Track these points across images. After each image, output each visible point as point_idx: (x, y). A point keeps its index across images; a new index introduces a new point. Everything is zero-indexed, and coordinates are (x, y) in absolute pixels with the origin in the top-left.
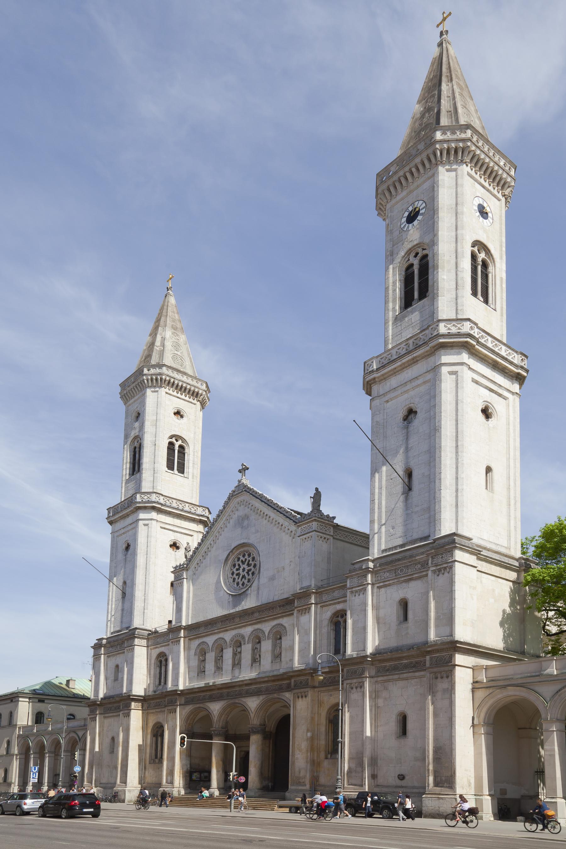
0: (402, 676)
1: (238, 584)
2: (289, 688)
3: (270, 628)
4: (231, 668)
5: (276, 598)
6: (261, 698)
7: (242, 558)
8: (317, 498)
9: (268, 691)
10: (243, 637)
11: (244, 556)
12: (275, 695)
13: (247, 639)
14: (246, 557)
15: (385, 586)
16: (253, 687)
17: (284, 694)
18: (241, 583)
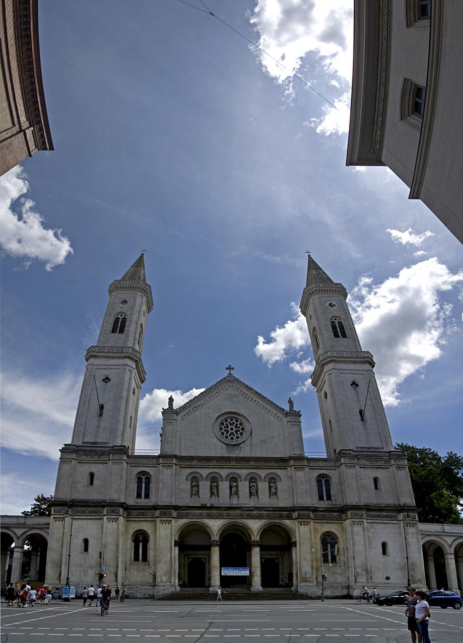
0: (383, 521)
1: (227, 437)
2: (289, 517)
3: (265, 474)
4: (229, 496)
6: (263, 521)
7: (229, 421)
9: (268, 517)
10: (240, 476)
11: (232, 420)
12: (277, 521)
13: (243, 478)
14: (234, 421)
15: (364, 468)
18: (229, 437)
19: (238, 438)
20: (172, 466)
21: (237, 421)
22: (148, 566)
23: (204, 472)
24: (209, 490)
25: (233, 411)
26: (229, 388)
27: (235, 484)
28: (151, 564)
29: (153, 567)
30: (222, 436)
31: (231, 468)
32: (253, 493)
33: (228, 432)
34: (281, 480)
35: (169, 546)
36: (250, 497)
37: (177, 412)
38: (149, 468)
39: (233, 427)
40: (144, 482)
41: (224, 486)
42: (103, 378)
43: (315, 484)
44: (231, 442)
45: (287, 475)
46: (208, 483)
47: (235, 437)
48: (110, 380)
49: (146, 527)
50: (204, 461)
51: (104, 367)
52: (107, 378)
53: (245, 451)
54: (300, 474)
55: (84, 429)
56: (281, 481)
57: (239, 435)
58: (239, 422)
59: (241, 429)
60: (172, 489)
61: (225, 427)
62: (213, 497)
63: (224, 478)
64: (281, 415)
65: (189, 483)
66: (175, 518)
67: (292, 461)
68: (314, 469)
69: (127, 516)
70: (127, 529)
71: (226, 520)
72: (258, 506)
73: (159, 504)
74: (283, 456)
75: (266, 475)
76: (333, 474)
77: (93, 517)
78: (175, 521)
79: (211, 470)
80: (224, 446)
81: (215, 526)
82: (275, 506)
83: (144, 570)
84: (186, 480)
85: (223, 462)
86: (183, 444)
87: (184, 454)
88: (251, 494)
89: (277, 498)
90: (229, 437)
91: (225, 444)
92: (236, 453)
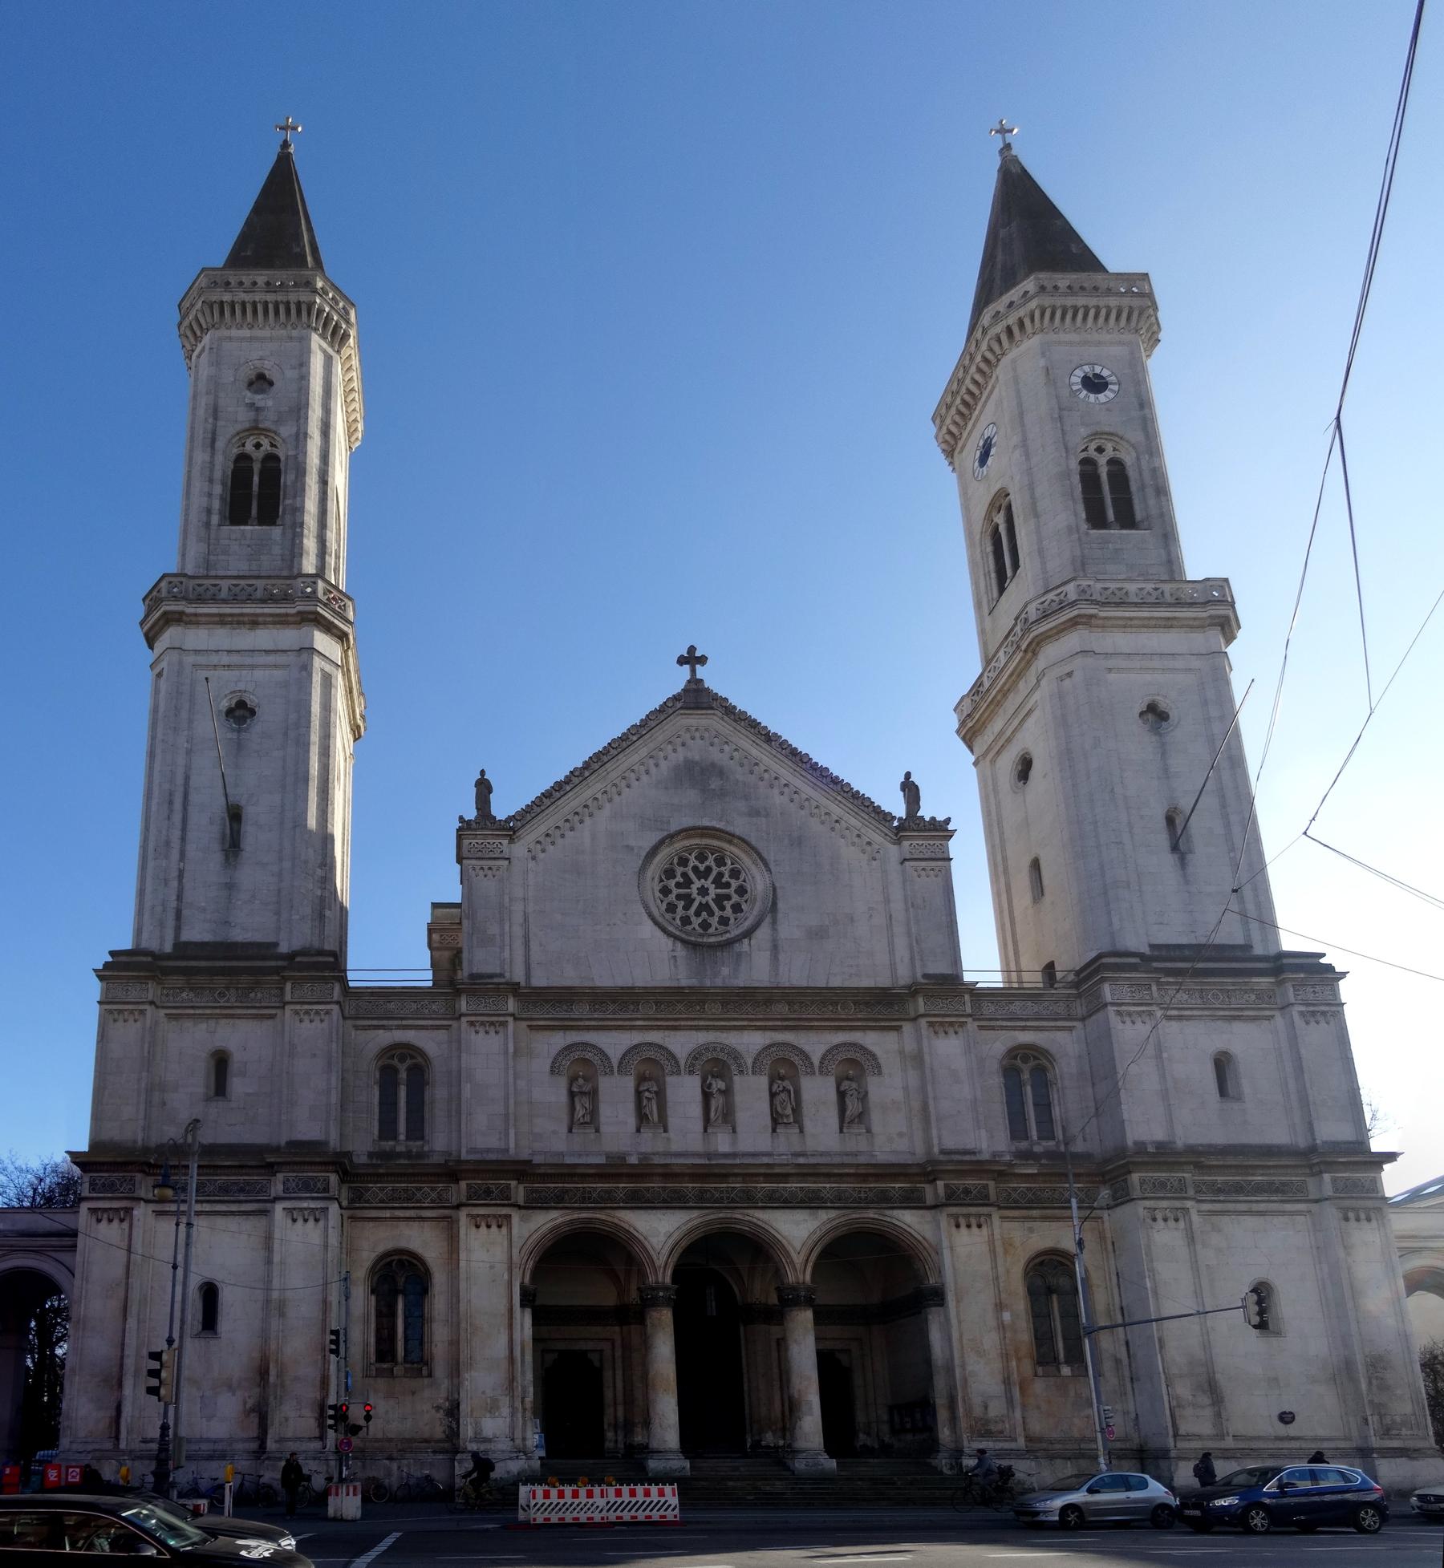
2: (913, 1201)
3: (827, 1047)
5: (836, 982)
6: (824, 1215)
7: (693, 862)
8: (910, 789)
9: (839, 1201)
10: (736, 1055)
11: (702, 858)
13: (750, 1062)
14: (710, 862)
16: (793, 1185)
17: (895, 1213)
18: (696, 922)
19: (724, 921)
20: (504, 1024)
21: (720, 862)
22: (426, 1381)
23: (615, 1043)
24: (631, 1106)
25: (706, 822)
26: (693, 738)
27: (721, 1085)
28: (440, 1370)
29: (445, 1385)
30: (669, 916)
31: (707, 1028)
32: (785, 1112)
33: (688, 900)
34: (879, 1066)
35: (502, 1307)
36: (774, 1130)
37: (511, 828)
38: (423, 1033)
39: (708, 883)
40: (404, 1079)
41: (685, 1092)
42: (225, 704)
43: (996, 1081)
44: (702, 935)
45: (901, 1052)
46: (629, 1083)
47: (714, 921)
48: (252, 712)
49: (421, 1239)
50: (611, 1007)
51: (226, 659)
52: (241, 704)
53: (755, 968)
54: (948, 1049)
55: (179, 898)
56: (880, 1073)
57: (728, 912)
58: (729, 866)
59: (736, 891)
60: (507, 1107)
61: (678, 885)
62: (647, 1134)
63: (682, 1063)
64: (878, 838)
65: (563, 1082)
66: (520, 1207)
67: (921, 1001)
68: (993, 1028)
69: (351, 1201)
70: (349, 1248)
71: (696, 1213)
72: (801, 1160)
73: (464, 1156)
74: (884, 981)
75: (829, 1051)
76: (1065, 1045)
77: (234, 1208)
78: (522, 1219)
79: (637, 1038)
80: (681, 951)
81: (660, 1232)
82: (862, 1160)
83: (413, 1393)
84: (552, 1071)
85: (679, 1006)
86: (534, 947)
87: (539, 980)
88: (776, 1120)
89: (869, 1131)
90: (696, 922)
91: (683, 941)
92: (726, 975)
